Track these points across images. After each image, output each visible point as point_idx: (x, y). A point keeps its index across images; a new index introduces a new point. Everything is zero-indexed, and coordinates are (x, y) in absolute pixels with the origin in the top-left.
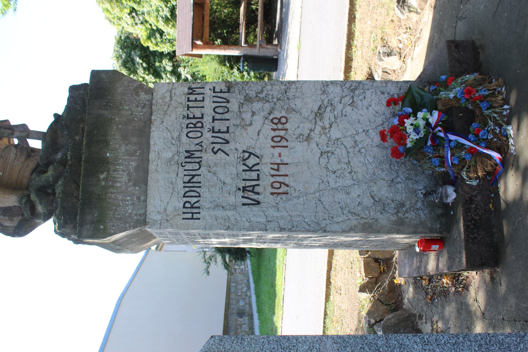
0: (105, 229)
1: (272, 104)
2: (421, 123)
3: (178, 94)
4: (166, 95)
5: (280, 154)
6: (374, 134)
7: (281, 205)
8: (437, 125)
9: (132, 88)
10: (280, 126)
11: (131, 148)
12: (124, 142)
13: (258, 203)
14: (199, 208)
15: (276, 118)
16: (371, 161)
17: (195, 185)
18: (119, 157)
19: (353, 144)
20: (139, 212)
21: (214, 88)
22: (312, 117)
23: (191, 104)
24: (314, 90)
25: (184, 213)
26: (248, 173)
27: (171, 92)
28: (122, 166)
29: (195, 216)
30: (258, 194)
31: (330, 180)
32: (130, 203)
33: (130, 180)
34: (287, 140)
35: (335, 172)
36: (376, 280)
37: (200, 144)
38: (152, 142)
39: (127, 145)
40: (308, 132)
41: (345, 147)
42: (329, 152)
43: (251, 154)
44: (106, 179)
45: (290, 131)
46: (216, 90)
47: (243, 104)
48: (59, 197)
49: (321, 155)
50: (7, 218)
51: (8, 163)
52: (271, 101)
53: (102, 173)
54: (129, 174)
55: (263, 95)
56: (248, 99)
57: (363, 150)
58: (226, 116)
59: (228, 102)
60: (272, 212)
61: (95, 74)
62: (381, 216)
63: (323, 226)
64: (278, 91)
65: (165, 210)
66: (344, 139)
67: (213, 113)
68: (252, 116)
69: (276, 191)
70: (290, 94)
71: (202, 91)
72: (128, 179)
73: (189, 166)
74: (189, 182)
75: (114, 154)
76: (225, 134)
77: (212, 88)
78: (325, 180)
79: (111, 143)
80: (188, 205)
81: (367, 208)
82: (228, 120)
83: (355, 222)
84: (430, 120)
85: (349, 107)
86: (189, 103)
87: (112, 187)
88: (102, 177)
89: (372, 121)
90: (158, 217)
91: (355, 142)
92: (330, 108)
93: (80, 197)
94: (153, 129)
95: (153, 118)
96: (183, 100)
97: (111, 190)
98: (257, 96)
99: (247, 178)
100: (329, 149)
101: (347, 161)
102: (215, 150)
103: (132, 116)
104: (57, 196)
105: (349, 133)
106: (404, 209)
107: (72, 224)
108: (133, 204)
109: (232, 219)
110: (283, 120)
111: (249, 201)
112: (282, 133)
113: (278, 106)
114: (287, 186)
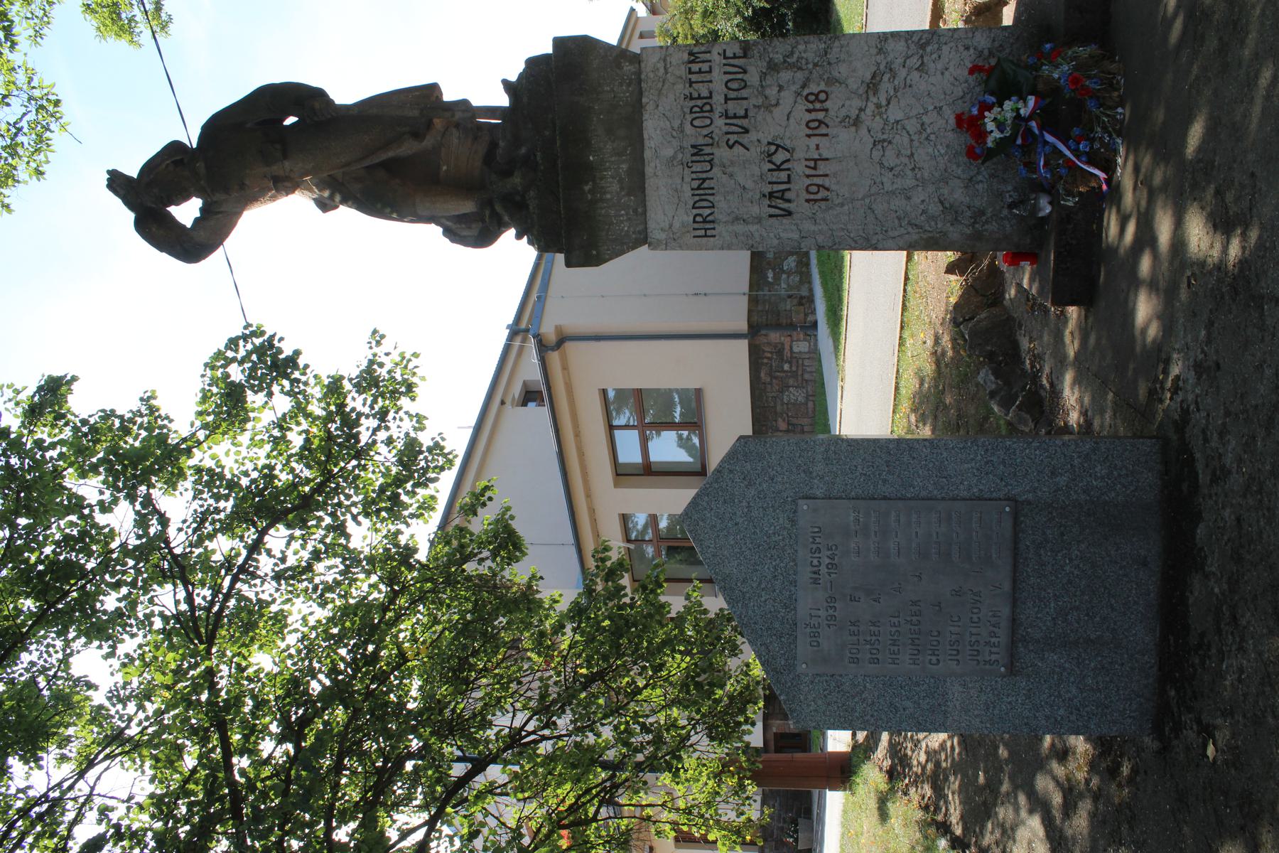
1: (807, 72)
2: (1009, 115)
3: (674, 63)
4: (659, 65)
5: (817, 146)
6: (949, 112)
7: (819, 215)
8: (1031, 117)
10: (818, 106)
13: (789, 213)
14: (713, 222)
15: (812, 94)
16: (943, 152)
17: (707, 192)
19: (919, 128)
21: (725, 51)
22: (861, 91)
23: (694, 77)
24: (866, 48)
25: (694, 229)
26: (775, 173)
27: (665, 60)
29: (709, 233)
30: (789, 201)
31: (885, 180)
33: (622, 188)
34: (827, 126)
35: (891, 169)
36: (972, 257)
38: (646, 136)
39: (613, 142)
40: (857, 112)
41: (908, 132)
42: (884, 140)
43: (778, 146)
44: (592, 191)
45: (832, 113)
46: (729, 54)
47: (765, 74)
49: (874, 145)
52: (804, 67)
53: (587, 183)
54: (621, 181)
55: (794, 59)
56: (773, 67)
57: (932, 137)
58: (744, 93)
59: (745, 72)
60: (808, 226)
61: (559, 43)
62: (951, 229)
63: (874, 242)
64: (815, 52)
65: (671, 226)
66: (906, 122)
67: (725, 90)
68: (779, 91)
69: (812, 197)
70: (832, 56)
71: (707, 56)
73: (698, 167)
74: (699, 188)
76: (743, 120)
77: (721, 52)
78: (878, 181)
80: (698, 219)
81: (933, 218)
82: (746, 99)
83: (915, 237)
84: (1022, 112)
85: (915, 73)
86: (690, 76)
88: (587, 188)
89: (949, 93)
90: (663, 236)
91: (923, 124)
92: (888, 75)
94: (646, 116)
95: (644, 100)
96: (682, 71)
98: (785, 61)
99: (774, 180)
100: (885, 137)
101: (909, 153)
102: (731, 143)
105: (914, 112)
106: (984, 218)
108: (629, 219)
109: (756, 235)
110: (822, 96)
111: (777, 212)
112: (821, 115)
113: (815, 74)
114: (828, 189)
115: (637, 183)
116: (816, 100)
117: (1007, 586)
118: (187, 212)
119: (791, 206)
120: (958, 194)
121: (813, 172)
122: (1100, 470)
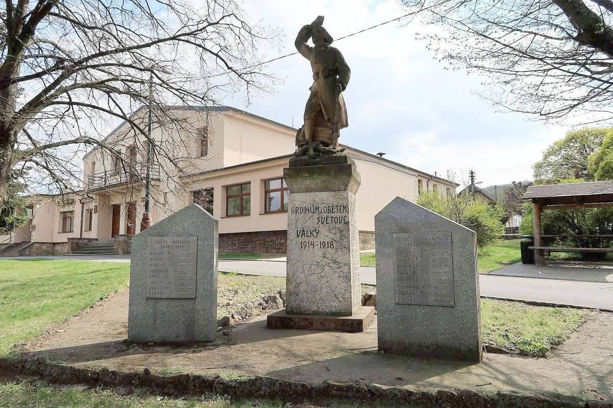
10: (329, 245)
13: (298, 237)
23: (339, 207)
37: (321, 212)
44: (305, 176)
56: (341, 231)
57: (319, 280)
58: (334, 223)
81: (296, 281)
88: (307, 174)
90: (292, 198)
96: (341, 204)
111: (299, 233)
115: (308, 190)
116: (331, 244)
117: (171, 297)
118: (310, 43)
119: (300, 237)
120: (303, 288)
121: (310, 244)
122: (204, 323)
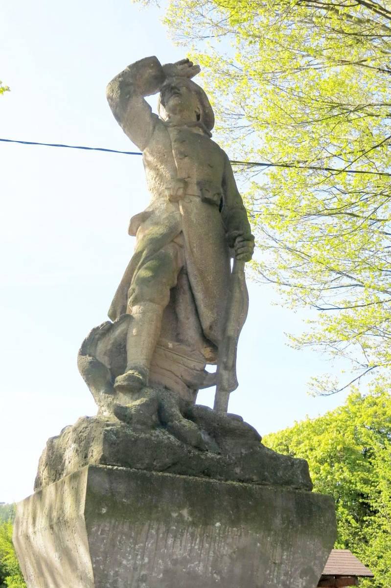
0: (100, 515)
9: (312, 563)
11: (225, 564)
12: (234, 552)
18: (213, 544)
20: (120, 580)
28: (199, 549)
32: (137, 562)
33: (175, 562)
39: (231, 557)
44: (180, 520)
48: (152, 435)
50: (109, 347)
51: (185, 357)
53: (191, 514)
54: (184, 561)
72: (177, 559)
75: (219, 534)
79: (234, 529)
87: (168, 531)
88: (185, 512)
93: (154, 473)
97: (163, 528)
103: (273, 565)
104: (152, 431)
107: (110, 454)
108: (135, 569)
